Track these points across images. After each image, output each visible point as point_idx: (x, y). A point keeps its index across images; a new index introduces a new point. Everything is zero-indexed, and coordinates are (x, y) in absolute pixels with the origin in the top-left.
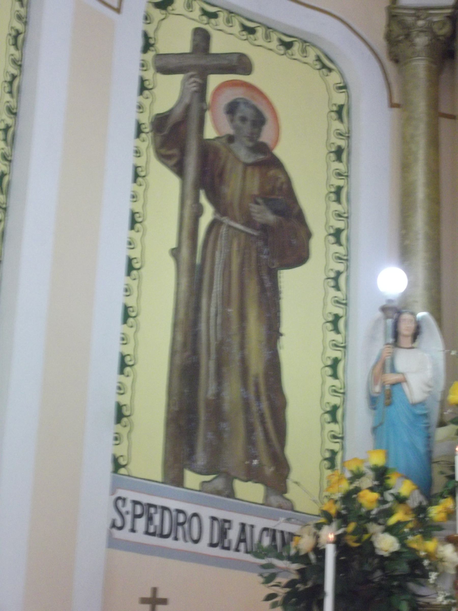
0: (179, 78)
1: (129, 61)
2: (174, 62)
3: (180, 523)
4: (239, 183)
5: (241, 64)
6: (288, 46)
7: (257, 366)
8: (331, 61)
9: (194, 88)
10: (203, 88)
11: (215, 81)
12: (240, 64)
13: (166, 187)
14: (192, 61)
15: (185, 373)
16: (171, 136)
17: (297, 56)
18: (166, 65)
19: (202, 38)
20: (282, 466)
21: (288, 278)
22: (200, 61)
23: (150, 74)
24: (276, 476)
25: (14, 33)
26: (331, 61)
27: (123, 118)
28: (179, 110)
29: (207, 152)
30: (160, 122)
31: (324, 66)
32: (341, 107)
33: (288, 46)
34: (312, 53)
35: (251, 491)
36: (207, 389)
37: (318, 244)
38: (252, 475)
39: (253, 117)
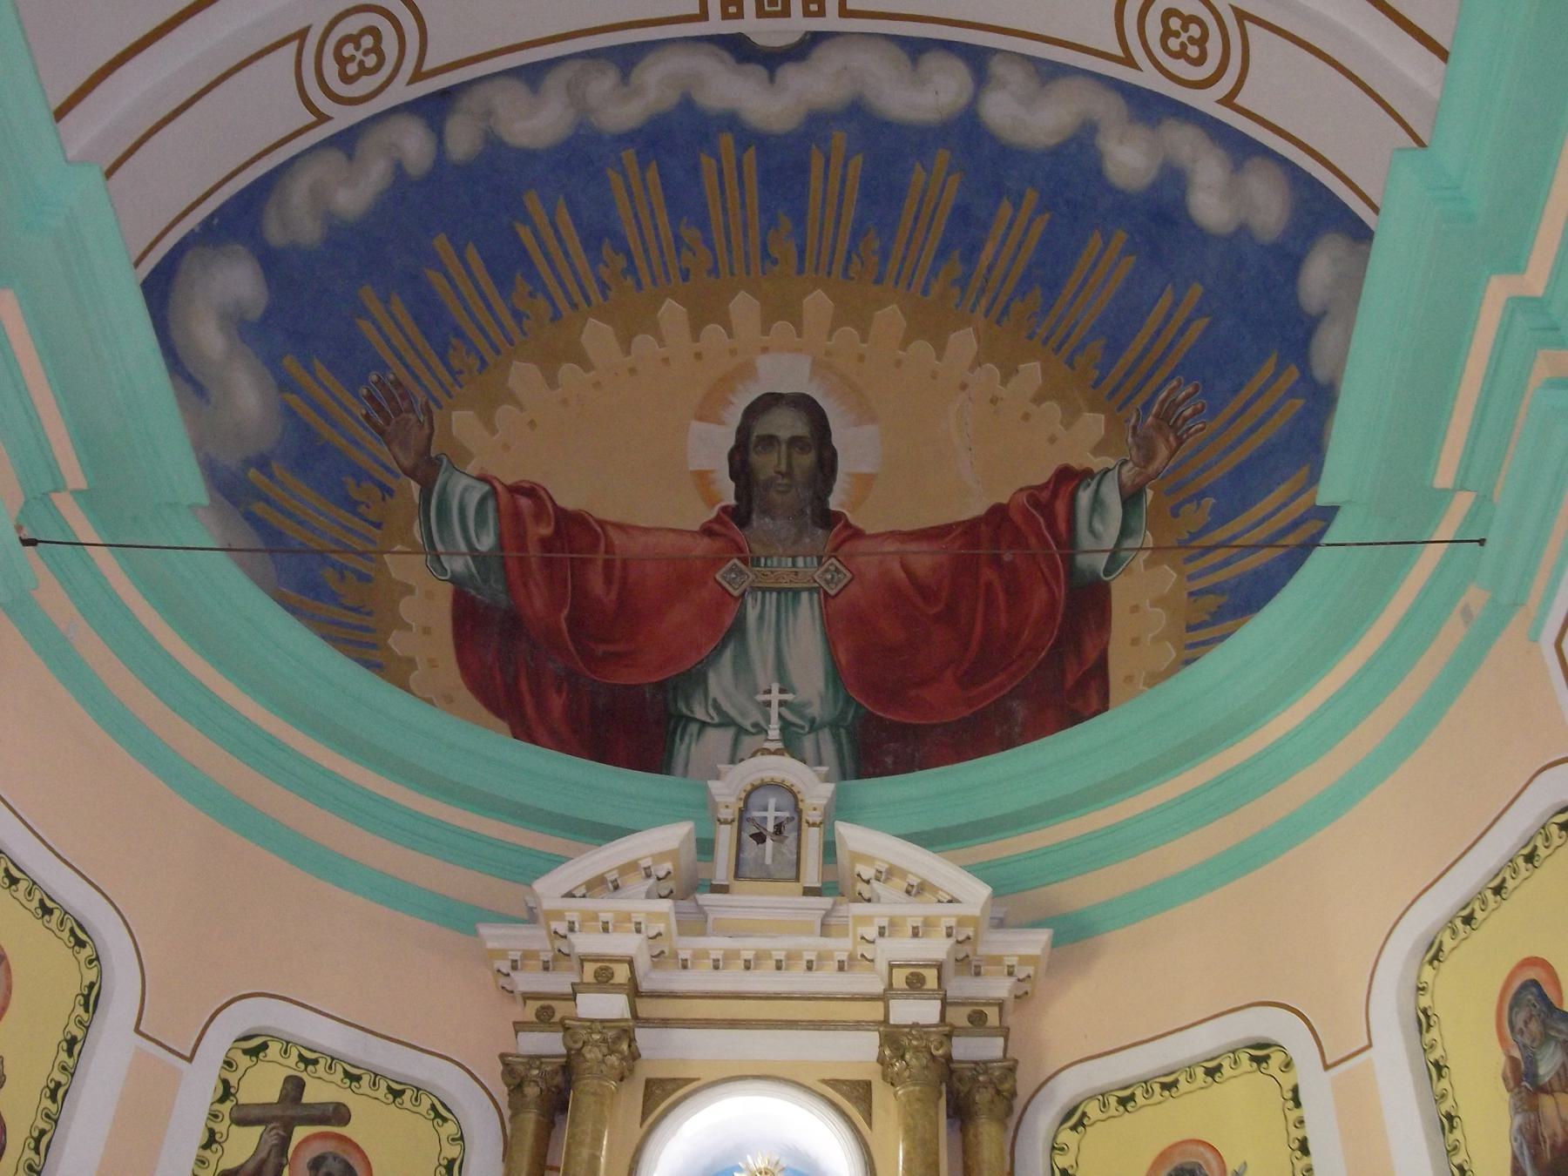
0: (259, 1129)
2: (256, 1113)
5: (340, 1114)
6: (397, 1094)
8: (449, 1110)
9: (273, 1140)
10: (286, 1141)
11: (300, 1133)
12: (340, 1114)
14: (279, 1113)
17: (407, 1104)
18: (243, 1118)
19: (295, 1086)
23: (221, 1127)
25: (52, 1085)
26: (449, 1110)
28: (251, 1167)
31: (438, 1115)
32: (452, 1162)
33: (397, 1094)
34: (426, 1102)
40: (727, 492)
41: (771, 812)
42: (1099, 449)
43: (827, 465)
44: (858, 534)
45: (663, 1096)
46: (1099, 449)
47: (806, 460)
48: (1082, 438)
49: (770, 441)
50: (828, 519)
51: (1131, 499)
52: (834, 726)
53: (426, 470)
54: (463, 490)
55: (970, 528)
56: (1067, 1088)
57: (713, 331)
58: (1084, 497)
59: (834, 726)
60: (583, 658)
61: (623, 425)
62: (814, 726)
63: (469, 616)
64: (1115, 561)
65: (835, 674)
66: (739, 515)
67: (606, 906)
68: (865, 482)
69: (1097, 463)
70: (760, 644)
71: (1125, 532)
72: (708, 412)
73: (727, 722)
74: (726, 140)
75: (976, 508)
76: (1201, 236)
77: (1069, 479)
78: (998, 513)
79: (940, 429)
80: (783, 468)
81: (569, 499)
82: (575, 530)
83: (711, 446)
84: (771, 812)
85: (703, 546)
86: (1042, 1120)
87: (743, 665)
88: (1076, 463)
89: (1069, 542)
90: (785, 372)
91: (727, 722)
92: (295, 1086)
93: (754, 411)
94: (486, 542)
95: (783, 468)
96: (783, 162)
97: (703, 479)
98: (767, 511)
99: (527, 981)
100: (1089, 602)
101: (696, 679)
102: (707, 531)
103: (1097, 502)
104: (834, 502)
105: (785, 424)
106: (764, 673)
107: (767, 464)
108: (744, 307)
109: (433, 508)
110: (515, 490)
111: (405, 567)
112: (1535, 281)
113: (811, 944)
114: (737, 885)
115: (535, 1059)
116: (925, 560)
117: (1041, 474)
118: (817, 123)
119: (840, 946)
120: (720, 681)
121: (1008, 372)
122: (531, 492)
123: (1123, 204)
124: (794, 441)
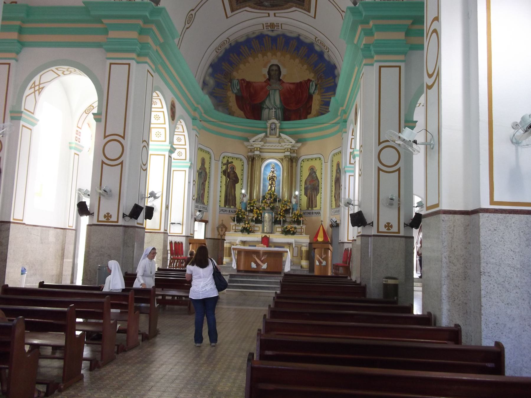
3: (226, 211)
5: (232, 162)
7: (233, 194)
12: (232, 162)
13: (224, 177)
15: (226, 196)
16: (225, 172)
18: (224, 165)
19: (228, 160)
20: (236, 204)
21: (237, 185)
22: (228, 163)
24: (235, 205)
27: (220, 171)
29: (228, 173)
30: (223, 171)
35: (232, 207)
36: (228, 198)
38: (232, 205)
39: (233, 168)
40: (267, 76)
42: (313, 78)
44: (283, 82)
45: (263, 160)
46: (313, 78)
47: (277, 73)
48: (311, 76)
49: (273, 70)
50: (280, 80)
51: (316, 85)
53: (231, 81)
54: (235, 82)
55: (297, 84)
56: (302, 158)
57: (265, 57)
58: (311, 83)
60: (251, 104)
61: (254, 70)
62: (278, 108)
63: (238, 98)
64: (314, 93)
65: (281, 101)
66: (269, 80)
67: (257, 143)
68: (285, 76)
69: (313, 80)
70: (272, 97)
71: (315, 89)
72: (265, 66)
73: (268, 108)
74: (267, 37)
75: (298, 81)
76: (325, 60)
77: (309, 80)
78: (301, 83)
79: (294, 72)
80: (274, 74)
81: (247, 80)
82: (249, 84)
83: (265, 71)
85: (264, 84)
86: (300, 161)
87: (270, 100)
88: (311, 78)
89: (309, 89)
90: (275, 61)
91: (268, 108)
92: (228, 160)
93: (271, 66)
94: (238, 88)
95: (274, 74)
96: (274, 39)
97: (264, 75)
99: (249, 147)
100: (310, 97)
101: (264, 102)
102: (265, 82)
103: (312, 85)
104: (281, 78)
105: (274, 68)
106: (272, 101)
107: (272, 73)
108: (269, 54)
110: (241, 80)
111: (230, 94)
112: (344, 108)
113: (277, 145)
114: (270, 136)
115: (251, 156)
116: (292, 86)
117: (306, 79)
118: (278, 36)
120: (267, 102)
121: (303, 66)
122: (243, 80)
123: (316, 52)
124: (276, 70)
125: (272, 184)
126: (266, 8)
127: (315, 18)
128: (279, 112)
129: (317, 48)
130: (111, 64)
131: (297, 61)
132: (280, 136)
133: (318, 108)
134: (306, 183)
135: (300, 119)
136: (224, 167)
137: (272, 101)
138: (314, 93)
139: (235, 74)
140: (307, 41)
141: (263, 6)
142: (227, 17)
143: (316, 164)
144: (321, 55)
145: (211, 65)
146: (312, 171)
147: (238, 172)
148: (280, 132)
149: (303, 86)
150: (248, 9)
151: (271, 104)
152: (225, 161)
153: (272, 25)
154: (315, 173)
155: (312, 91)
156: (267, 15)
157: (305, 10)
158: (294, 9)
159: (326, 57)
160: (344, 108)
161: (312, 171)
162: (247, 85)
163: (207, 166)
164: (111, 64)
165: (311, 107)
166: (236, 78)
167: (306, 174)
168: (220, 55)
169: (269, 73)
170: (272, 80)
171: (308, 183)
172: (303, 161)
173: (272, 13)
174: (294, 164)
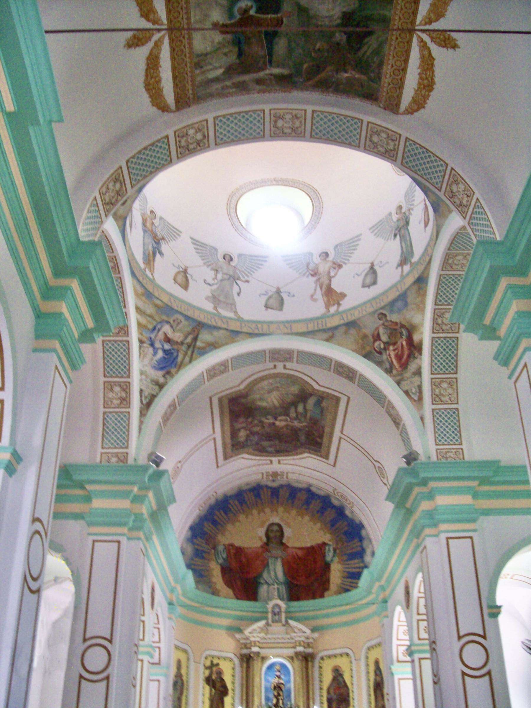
1: (202, 668)
4: (218, 685)
5: (218, 664)
12: (218, 664)
13: (207, 688)
16: (208, 680)
19: (212, 662)
22: (212, 665)
27: (202, 678)
29: (213, 681)
37: (230, 692)
39: (220, 673)
40: (265, 539)
41: (277, 610)
43: (282, 535)
44: (287, 547)
46: (330, 541)
47: (278, 534)
48: (326, 537)
49: (272, 531)
51: (335, 550)
52: (284, 583)
54: (221, 548)
55: (307, 548)
57: (262, 514)
58: (327, 548)
59: (284, 583)
64: (332, 560)
66: (267, 544)
67: (255, 635)
69: (329, 543)
70: (271, 567)
71: (334, 556)
72: (262, 526)
73: (267, 583)
74: (265, 489)
75: (308, 545)
76: (346, 517)
77: (324, 544)
78: (312, 548)
79: (303, 532)
80: (275, 536)
83: (261, 532)
84: (277, 610)
89: (324, 556)
90: (276, 519)
92: (212, 662)
94: (225, 556)
95: (275, 536)
96: (275, 492)
97: (261, 539)
98: (272, 543)
99: (242, 641)
100: (327, 567)
102: (262, 547)
103: (329, 550)
105: (275, 528)
106: (272, 573)
107: (271, 535)
108: (267, 510)
109: (217, 554)
112: (383, 582)
116: (300, 553)
117: (320, 542)
118: (282, 486)
119: (289, 636)
120: (265, 575)
122: (232, 545)
123: (333, 507)
125: (279, 694)
126: (270, 454)
127: (334, 466)
128: (283, 589)
129: (335, 502)
130: (94, 541)
131: (307, 518)
132: (287, 622)
133: (339, 581)
134: (328, 692)
135: (314, 598)
136: (207, 672)
137: (272, 573)
138: (332, 560)
139: (220, 537)
140: (322, 493)
141: (267, 452)
142: (218, 466)
143: (343, 663)
144: (340, 511)
145: (192, 528)
146: (337, 673)
147: (227, 678)
148: (287, 618)
149: (315, 553)
150: (246, 456)
151: (271, 577)
152: (208, 663)
153: (275, 475)
154: (341, 675)
155: (328, 558)
156: (269, 462)
157: (321, 456)
158: (306, 455)
159: (347, 513)
160: (383, 582)
161: (337, 673)
162: (237, 552)
163: (183, 671)
164: (94, 541)
165: (328, 581)
166: (222, 543)
167: (328, 678)
168: (203, 513)
169: (267, 535)
170: (271, 545)
171: (332, 691)
172: (322, 658)
173: (275, 459)
174: (310, 664)
